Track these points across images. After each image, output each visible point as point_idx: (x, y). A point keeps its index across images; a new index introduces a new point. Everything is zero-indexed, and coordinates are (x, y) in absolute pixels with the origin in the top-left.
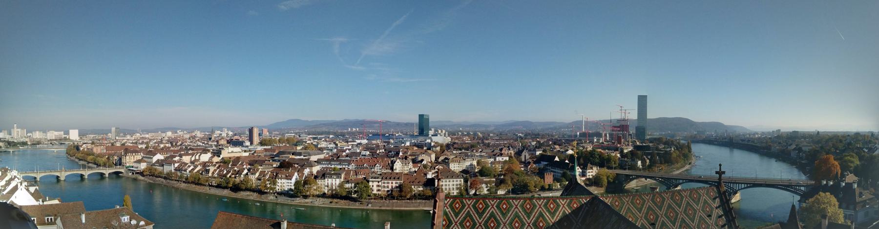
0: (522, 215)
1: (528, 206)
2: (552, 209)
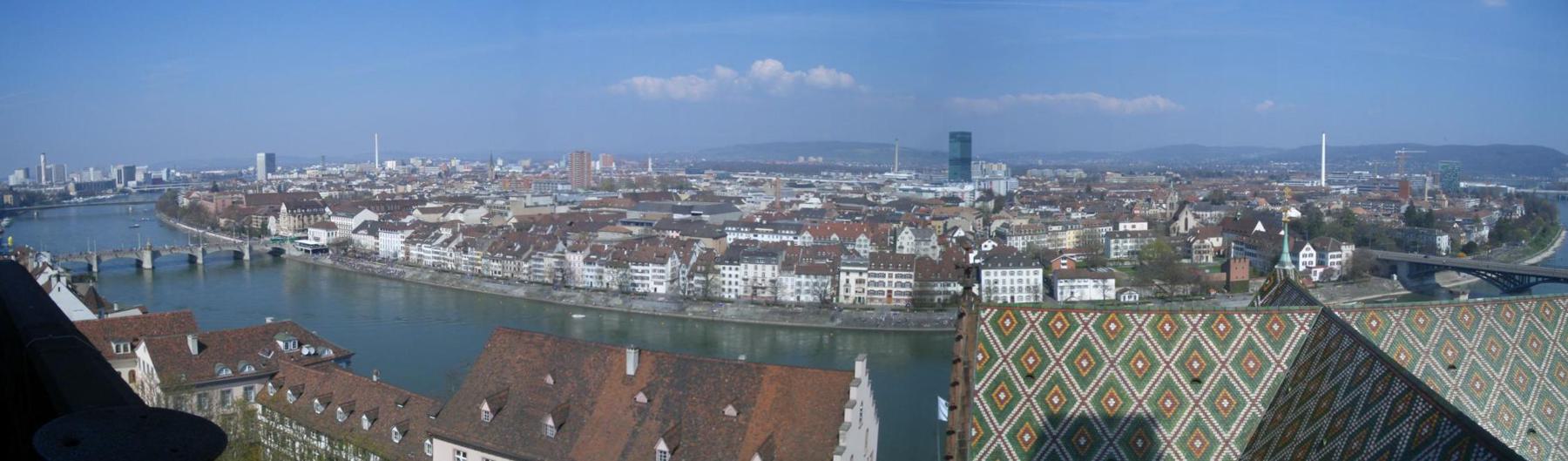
0: (1153, 345)
1: (1167, 327)
2: (1222, 333)
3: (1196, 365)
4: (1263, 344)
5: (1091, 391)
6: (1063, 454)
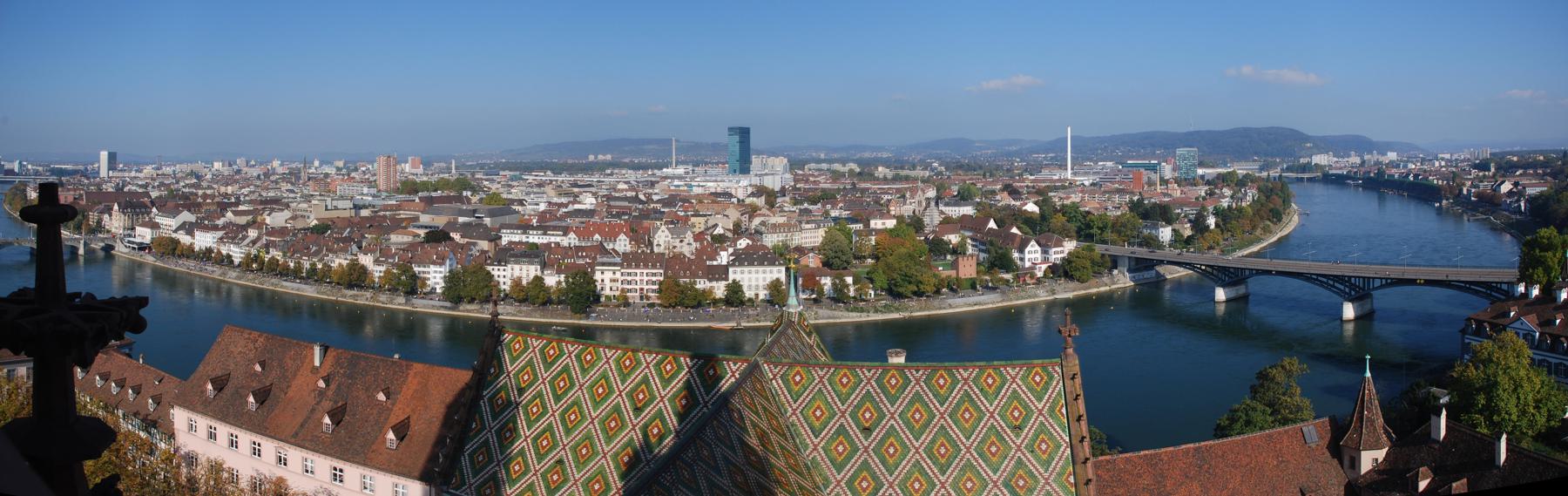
2: (667, 372)
3: (641, 396)
4: (697, 386)
5: (561, 407)
6: (529, 450)
